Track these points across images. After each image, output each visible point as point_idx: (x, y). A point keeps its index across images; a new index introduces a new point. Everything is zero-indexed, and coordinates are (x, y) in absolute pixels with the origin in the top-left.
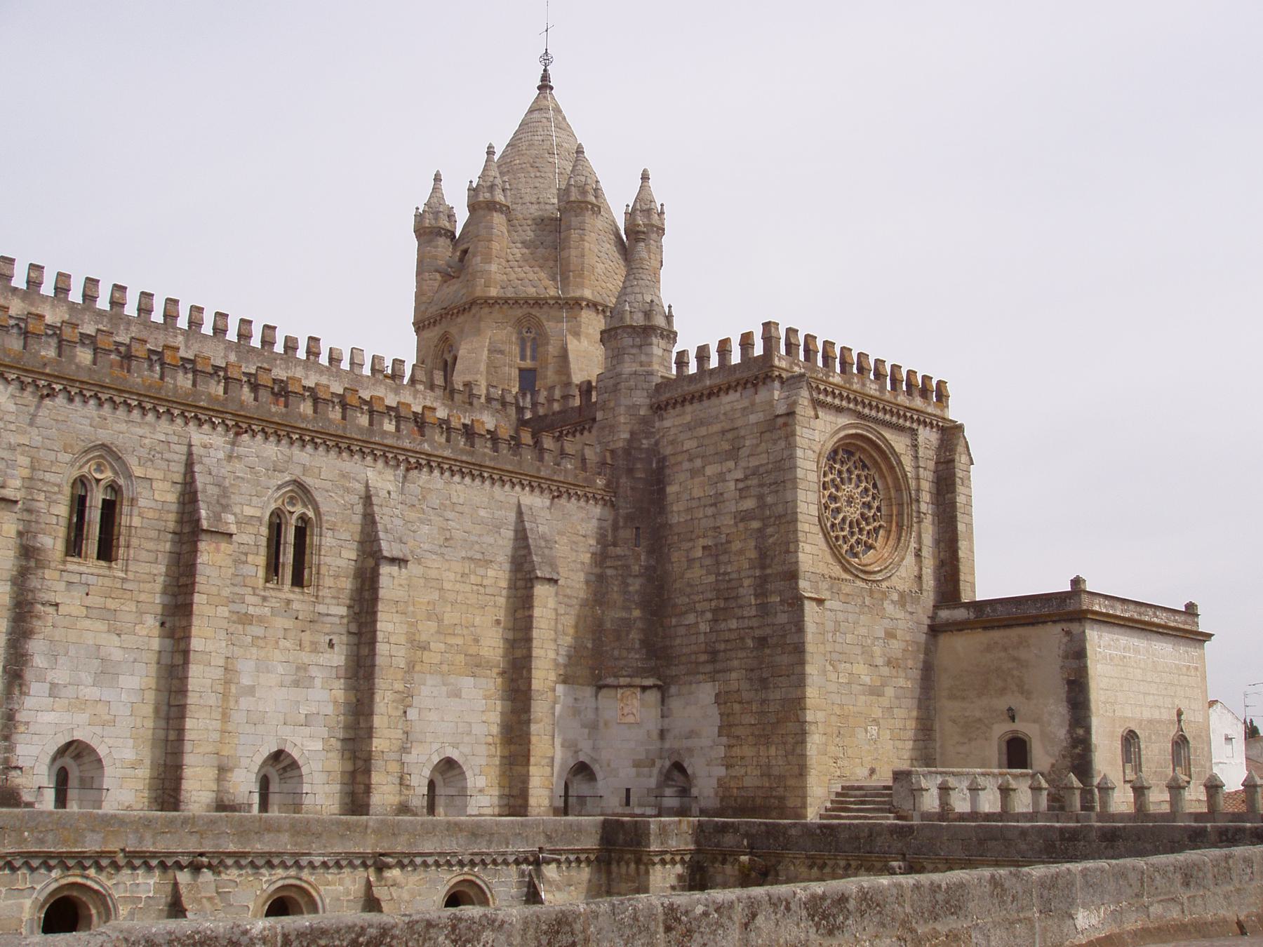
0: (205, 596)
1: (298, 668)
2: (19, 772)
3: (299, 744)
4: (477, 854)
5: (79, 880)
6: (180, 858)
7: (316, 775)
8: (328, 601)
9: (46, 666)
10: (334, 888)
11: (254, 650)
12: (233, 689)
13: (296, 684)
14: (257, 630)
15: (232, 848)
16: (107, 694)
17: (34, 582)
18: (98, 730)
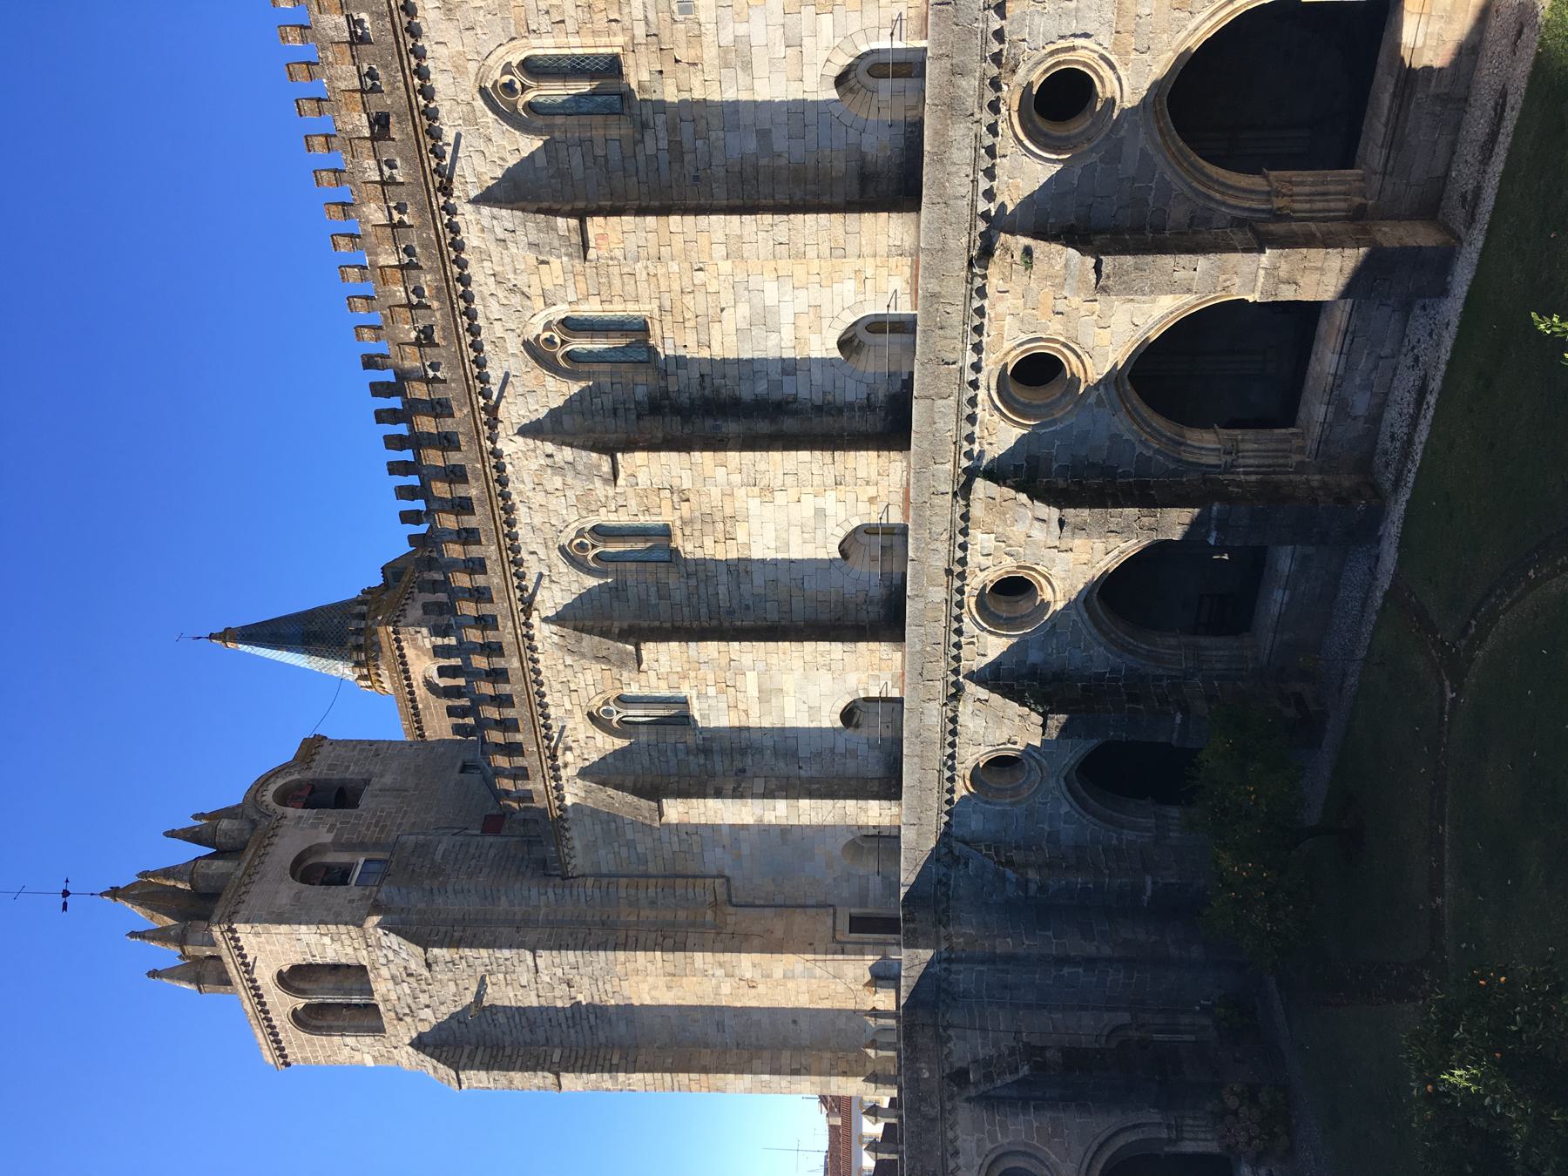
0: (662, 249)
1: (727, 65)
2: (872, 396)
3: (825, 55)
4: (982, 96)
5: (973, 600)
6: (957, 516)
7: (867, 23)
8: (628, 24)
9: (765, 381)
10: (1006, 327)
11: (713, 135)
12: (764, 162)
13: (747, 66)
14: (687, 130)
15: (949, 466)
16: (787, 317)
17: (684, 398)
18: (826, 323)
